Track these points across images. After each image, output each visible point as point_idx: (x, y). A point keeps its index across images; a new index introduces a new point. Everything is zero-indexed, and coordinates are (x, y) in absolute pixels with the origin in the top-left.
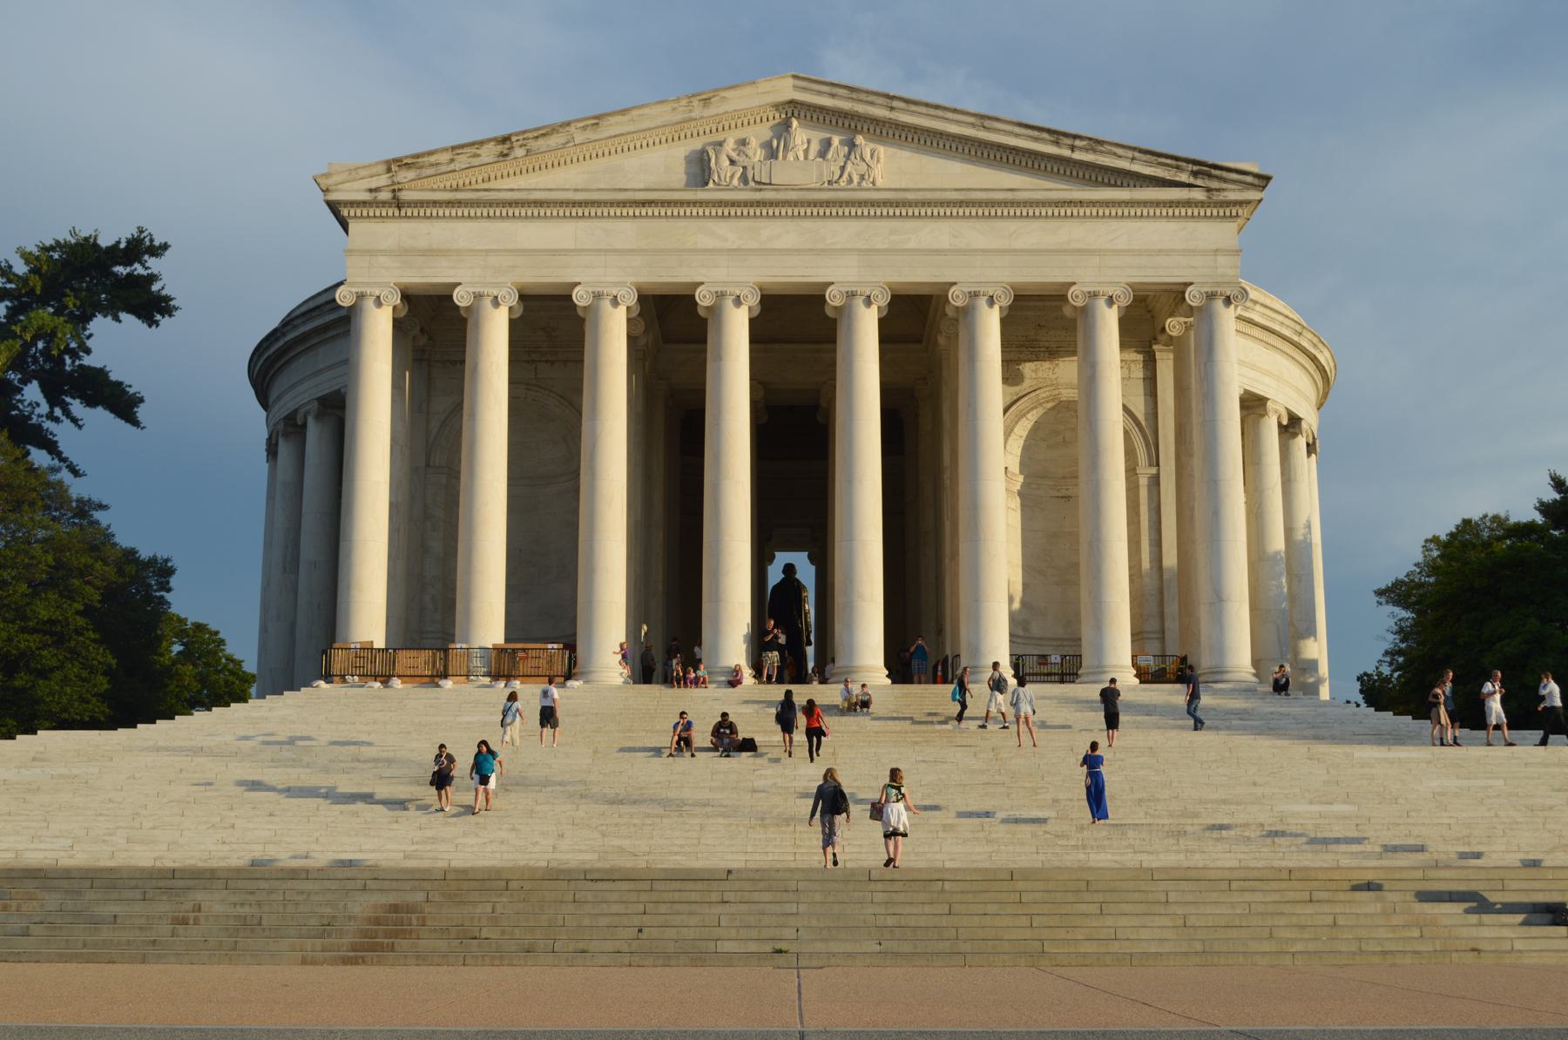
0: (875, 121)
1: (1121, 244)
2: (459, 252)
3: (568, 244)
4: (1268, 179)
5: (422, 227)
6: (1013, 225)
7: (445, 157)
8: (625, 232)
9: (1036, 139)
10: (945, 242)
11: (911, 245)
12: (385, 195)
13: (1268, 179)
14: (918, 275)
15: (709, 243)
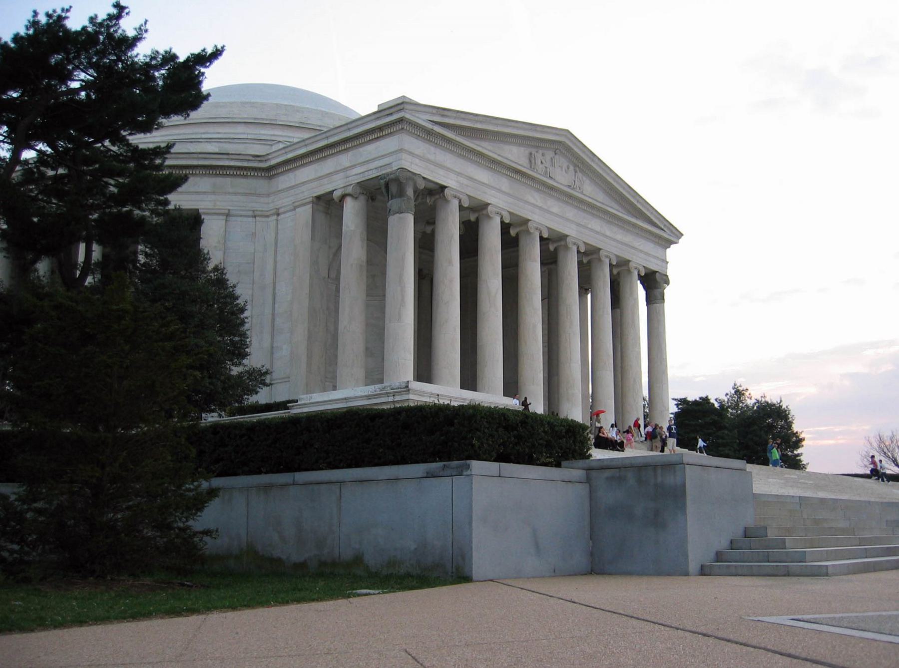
0: (583, 162)
1: (641, 248)
2: (448, 169)
3: (486, 181)
4: (682, 235)
5: (432, 149)
6: (615, 229)
7: (454, 115)
8: (504, 183)
9: (629, 193)
10: (598, 228)
11: (590, 226)
12: (430, 126)
13: (682, 235)
14: (595, 242)
15: (532, 201)
